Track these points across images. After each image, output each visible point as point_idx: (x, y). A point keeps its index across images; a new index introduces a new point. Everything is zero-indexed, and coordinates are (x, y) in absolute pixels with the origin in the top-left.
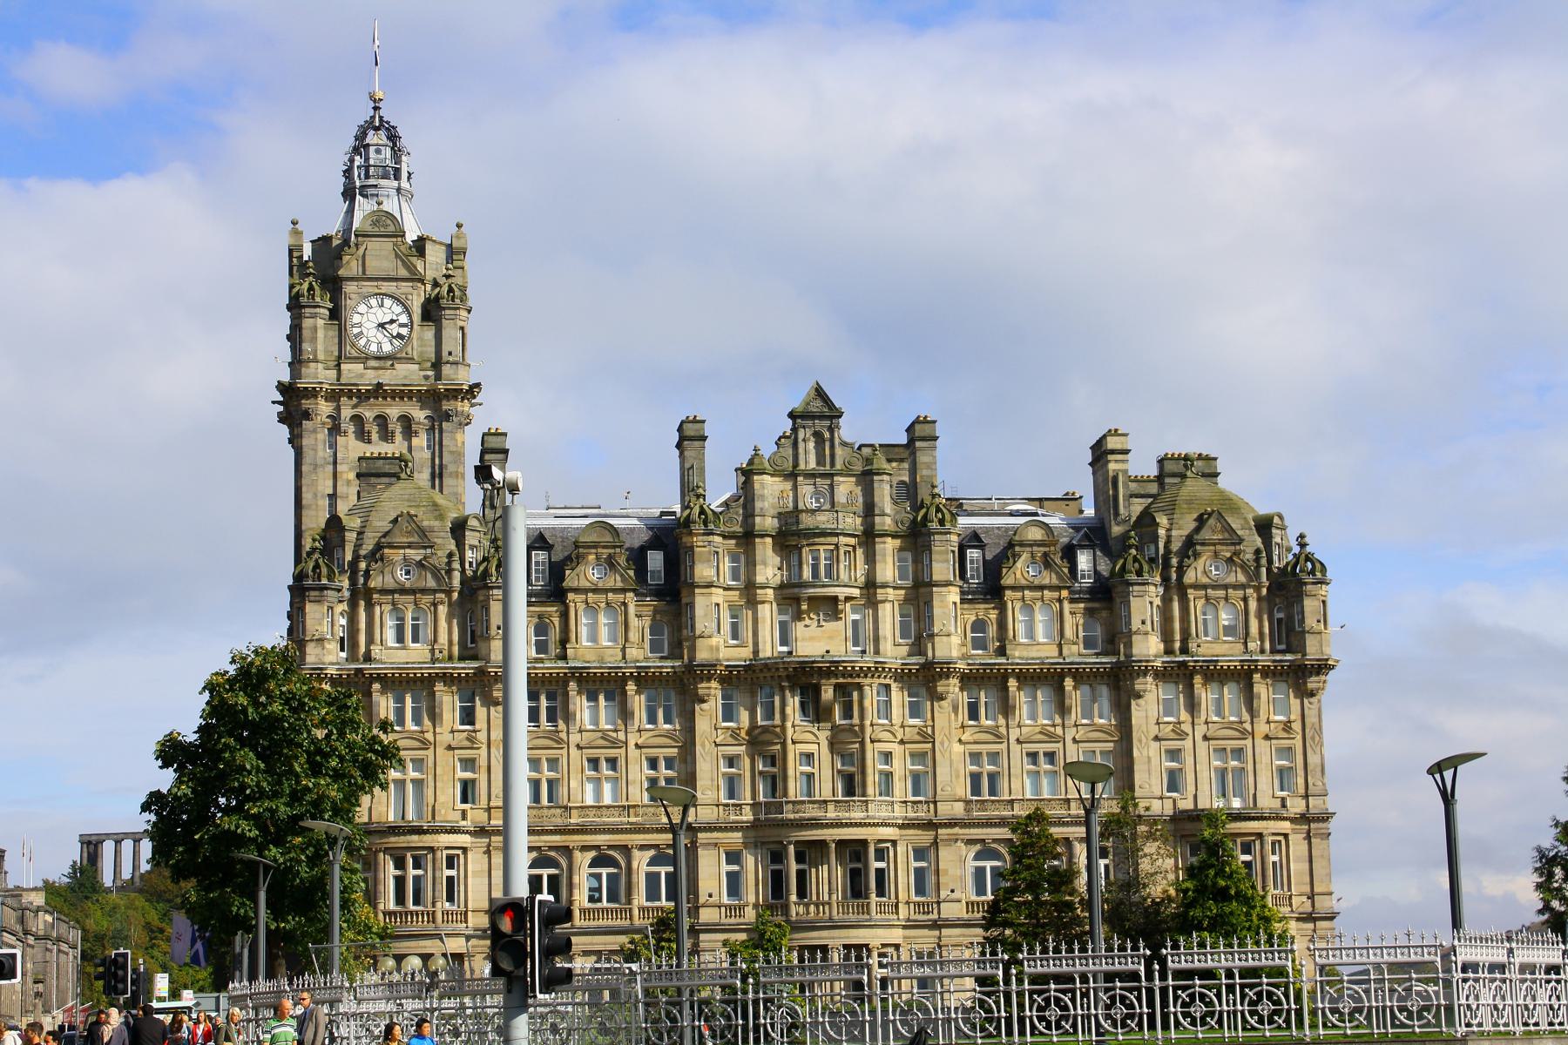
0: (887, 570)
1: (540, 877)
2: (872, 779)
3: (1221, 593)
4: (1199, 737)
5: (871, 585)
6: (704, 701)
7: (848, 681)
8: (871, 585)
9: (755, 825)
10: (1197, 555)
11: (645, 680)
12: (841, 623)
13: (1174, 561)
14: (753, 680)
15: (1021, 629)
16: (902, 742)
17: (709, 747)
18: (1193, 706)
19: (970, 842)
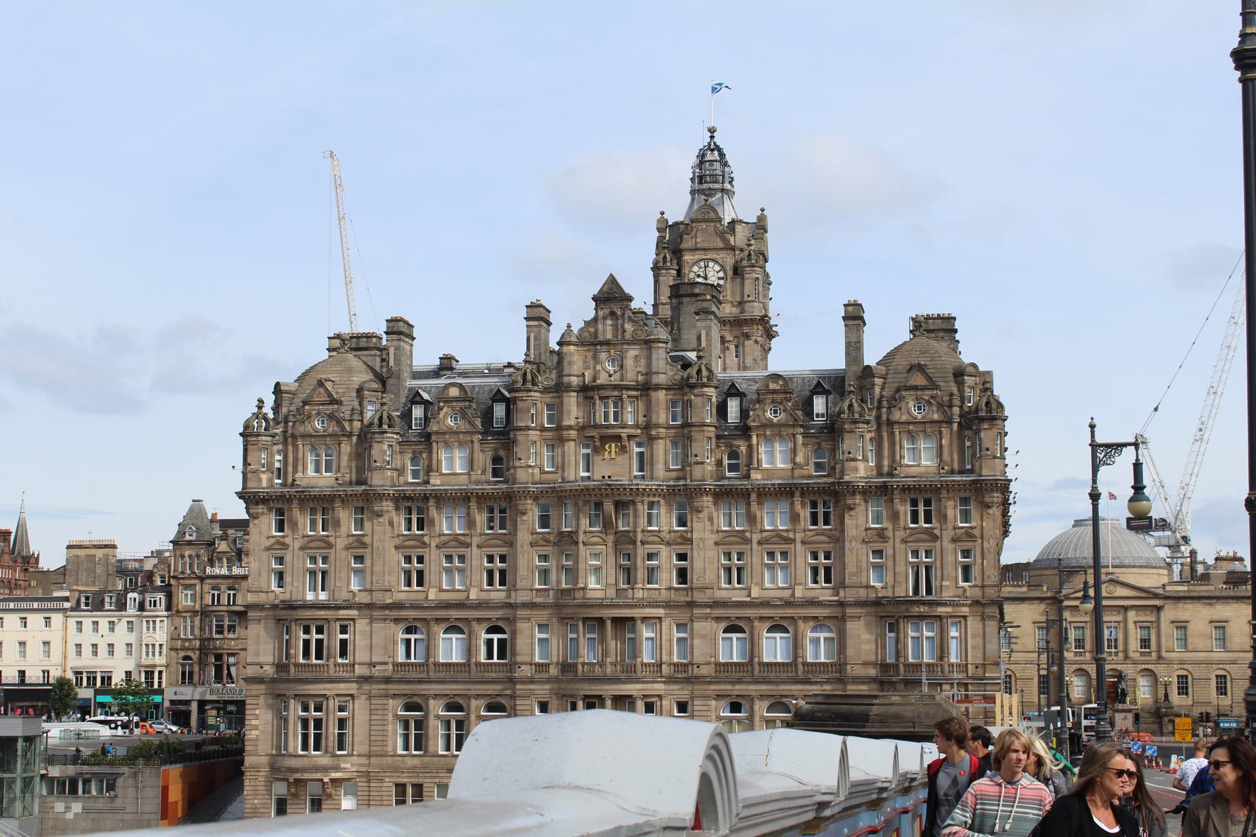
0: (662, 416)
1: (408, 641)
2: (641, 574)
3: (921, 427)
4: (898, 541)
5: (647, 427)
6: (524, 514)
7: (624, 500)
8: (647, 427)
9: (557, 606)
10: (902, 398)
11: (482, 498)
13: (885, 404)
14: (555, 497)
15: (763, 457)
16: (668, 544)
17: (527, 547)
18: (895, 516)
19: (718, 619)
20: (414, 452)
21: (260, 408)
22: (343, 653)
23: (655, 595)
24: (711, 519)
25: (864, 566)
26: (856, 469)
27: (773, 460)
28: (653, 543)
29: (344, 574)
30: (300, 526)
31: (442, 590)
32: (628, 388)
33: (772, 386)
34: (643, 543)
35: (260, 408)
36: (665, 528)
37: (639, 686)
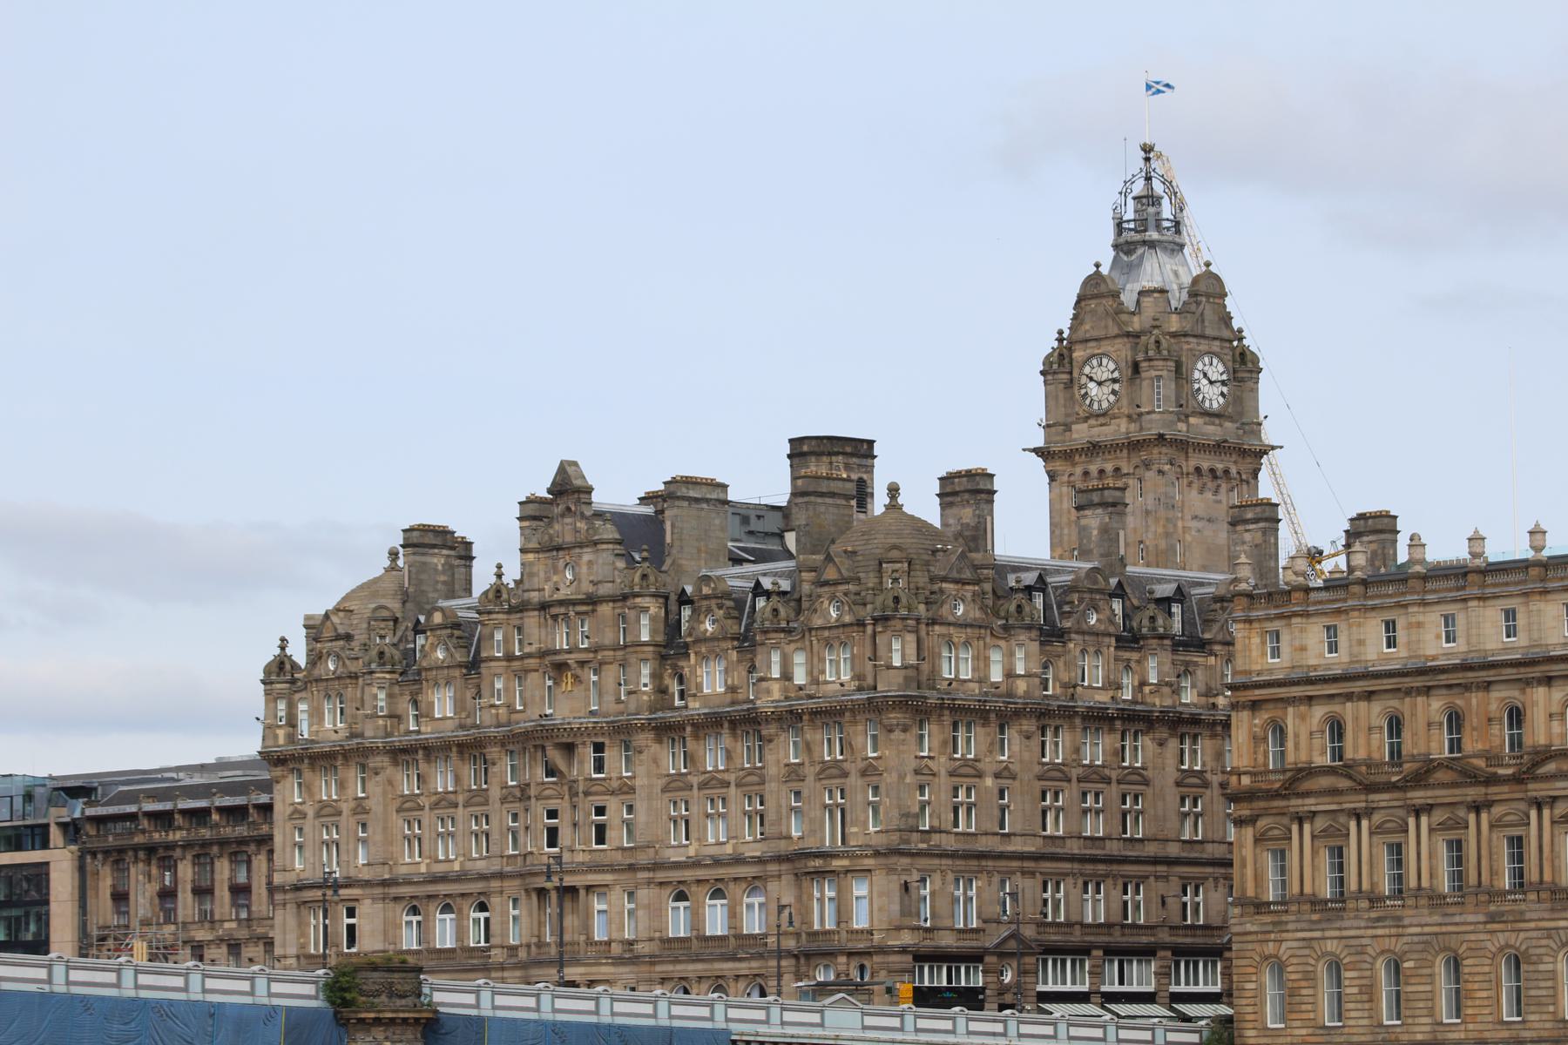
3: (835, 632)
12: (582, 687)
20: (411, 693)
21: (283, 648)
22: (352, 940)
23: (598, 858)
24: (655, 761)
25: (784, 811)
26: (768, 692)
27: (712, 680)
28: (596, 794)
29: (351, 846)
30: (316, 790)
31: (438, 861)
32: (574, 603)
33: (706, 590)
34: (586, 794)
35: (283, 648)
36: (614, 775)
37: (581, 970)
